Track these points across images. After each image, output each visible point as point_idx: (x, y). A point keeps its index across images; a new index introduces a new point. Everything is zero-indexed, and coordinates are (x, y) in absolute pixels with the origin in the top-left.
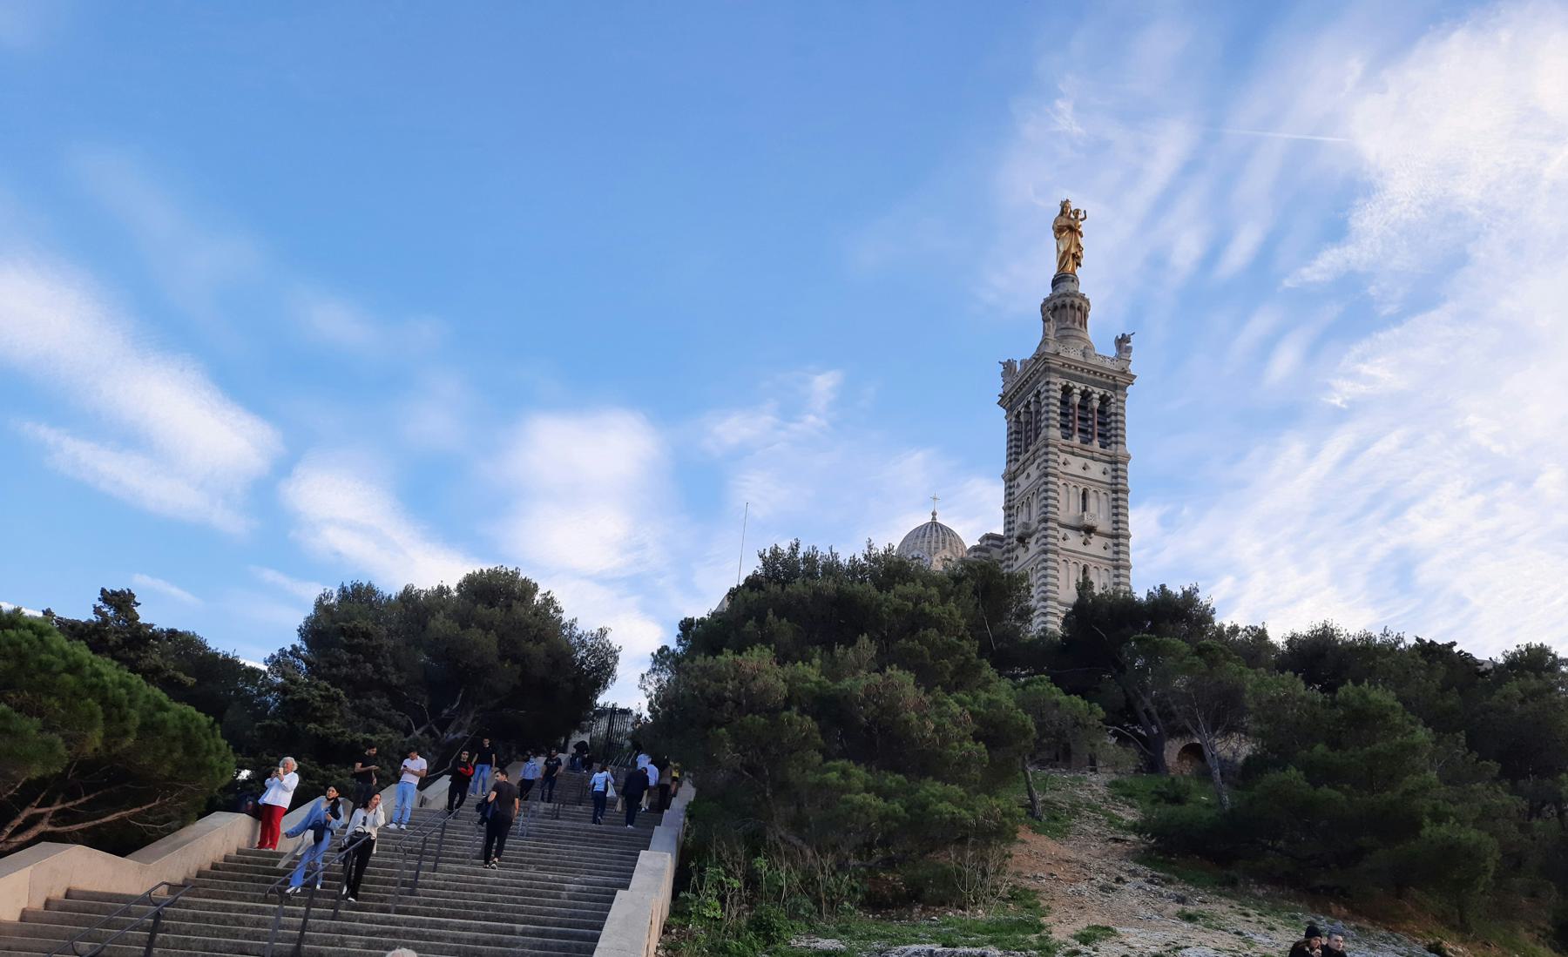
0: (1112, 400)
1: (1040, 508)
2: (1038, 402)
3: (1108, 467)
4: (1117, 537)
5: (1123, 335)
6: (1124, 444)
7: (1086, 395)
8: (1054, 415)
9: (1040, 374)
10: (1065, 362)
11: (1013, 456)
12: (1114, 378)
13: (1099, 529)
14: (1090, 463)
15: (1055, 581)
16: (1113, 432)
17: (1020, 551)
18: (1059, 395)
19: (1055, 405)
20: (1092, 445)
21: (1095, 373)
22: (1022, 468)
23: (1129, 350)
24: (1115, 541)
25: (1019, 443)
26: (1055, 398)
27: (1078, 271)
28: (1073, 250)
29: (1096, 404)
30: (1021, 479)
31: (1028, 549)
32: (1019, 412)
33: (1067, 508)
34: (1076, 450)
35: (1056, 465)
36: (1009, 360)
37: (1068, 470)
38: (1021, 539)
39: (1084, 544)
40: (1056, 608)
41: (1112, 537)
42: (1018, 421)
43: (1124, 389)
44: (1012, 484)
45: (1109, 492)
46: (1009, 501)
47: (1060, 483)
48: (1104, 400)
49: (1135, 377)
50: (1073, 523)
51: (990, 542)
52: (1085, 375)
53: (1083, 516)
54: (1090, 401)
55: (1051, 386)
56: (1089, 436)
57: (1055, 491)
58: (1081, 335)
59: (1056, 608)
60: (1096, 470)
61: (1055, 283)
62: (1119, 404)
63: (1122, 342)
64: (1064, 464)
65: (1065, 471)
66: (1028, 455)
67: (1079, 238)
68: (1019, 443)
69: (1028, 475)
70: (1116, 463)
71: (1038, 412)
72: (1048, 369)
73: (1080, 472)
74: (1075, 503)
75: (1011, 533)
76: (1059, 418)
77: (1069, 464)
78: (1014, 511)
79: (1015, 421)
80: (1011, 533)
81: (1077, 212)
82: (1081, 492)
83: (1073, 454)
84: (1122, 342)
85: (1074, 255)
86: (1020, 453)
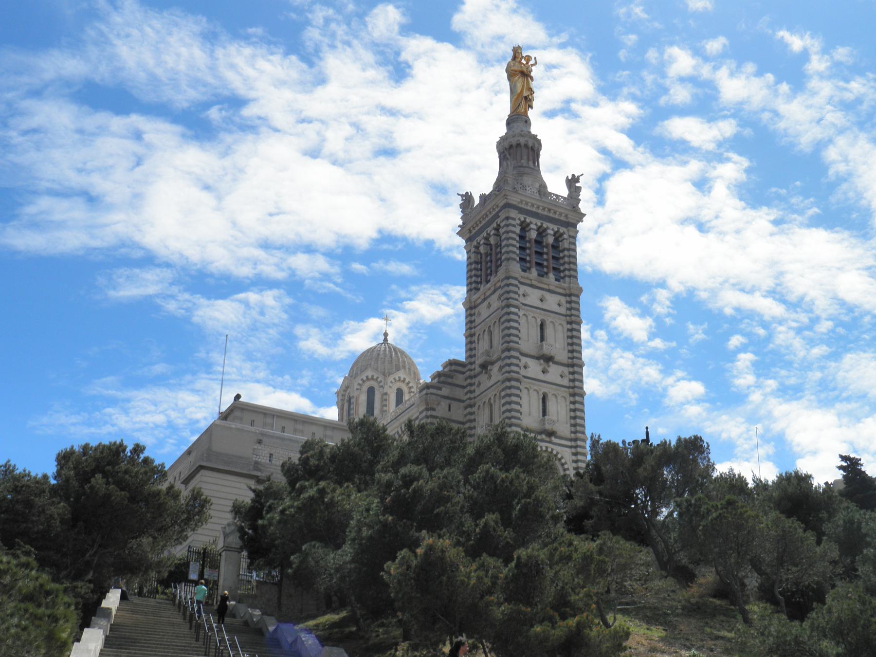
0: (565, 236)
1: (503, 337)
2: (497, 235)
3: (563, 299)
4: (573, 366)
5: (573, 175)
6: (576, 277)
7: (541, 232)
8: (515, 249)
9: (499, 209)
10: (523, 198)
11: (473, 285)
12: (566, 216)
13: (557, 358)
14: (548, 295)
15: (518, 407)
16: (567, 266)
17: (483, 378)
18: (518, 230)
19: (514, 239)
20: (549, 278)
21: (549, 210)
22: (482, 297)
23: (579, 188)
24: (571, 370)
25: (479, 273)
26: (514, 232)
28: (525, 94)
31: (490, 377)
32: (479, 243)
33: (528, 339)
34: (534, 283)
35: (516, 296)
36: (467, 193)
37: (528, 301)
38: (484, 366)
39: (543, 372)
41: (568, 366)
42: (477, 252)
43: (575, 226)
44: (473, 311)
45: (564, 323)
46: (471, 328)
47: (521, 313)
48: (558, 237)
49: (585, 215)
50: (533, 352)
51: (453, 367)
52: (540, 211)
53: (542, 346)
54: (545, 236)
55: (511, 221)
56: (545, 270)
57: (517, 321)
60: (552, 302)
61: (509, 123)
62: (572, 240)
63: (572, 182)
64: (524, 295)
65: (524, 302)
66: (489, 285)
67: (530, 81)
68: (479, 273)
69: (489, 306)
70: (570, 295)
71: (499, 245)
72: (508, 206)
73: (538, 304)
74: (535, 333)
75: (473, 360)
76: (518, 252)
77: (528, 295)
78: (475, 338)
79: (474, 252)
80: (473, 360)
82: (539, 323)
83: (532, 286)
84: (572, 182)
85: (526, 98)
86: (481, 283)
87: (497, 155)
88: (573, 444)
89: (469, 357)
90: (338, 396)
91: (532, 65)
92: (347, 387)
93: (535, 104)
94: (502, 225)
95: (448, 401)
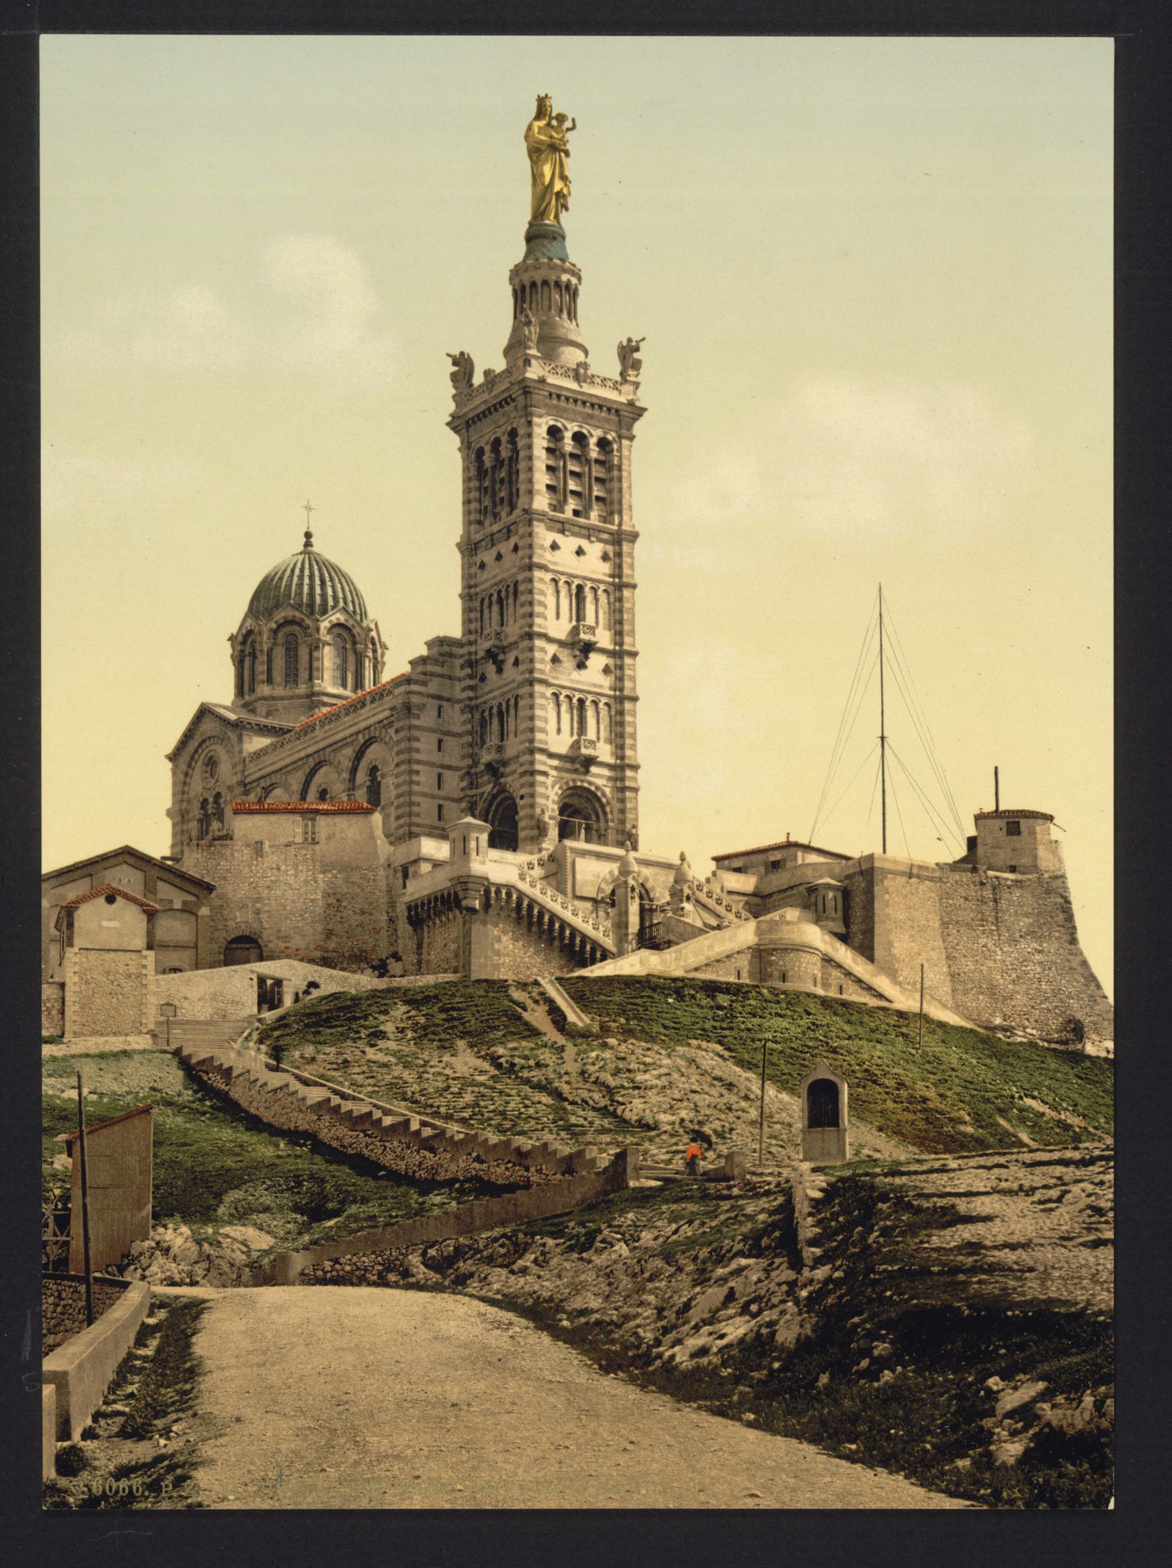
5: (630, 340)
7: (579, 438)
27: (563, 216)
29: (594, 452)
30: (488, 556)
31: (500, 671)
36: (462, 354)
40: (545, 764)
48: (603, 443)
49: (645, 410)
58: (572, 337)
59: (545, 764)
61: (529, 238)
69: (499, 557)
81: (561, 118)
85: (559, 195)
87: (508, 290)
88: (619, 774)
89: (467, 632)
90: (233, 646)
91: (568, 130)
92: (250, 632)
93: (571, 202)
94: (521, 431)
95: (436, 702)
